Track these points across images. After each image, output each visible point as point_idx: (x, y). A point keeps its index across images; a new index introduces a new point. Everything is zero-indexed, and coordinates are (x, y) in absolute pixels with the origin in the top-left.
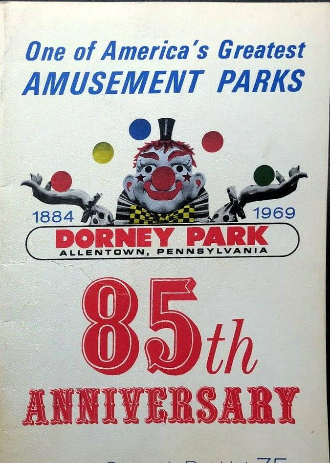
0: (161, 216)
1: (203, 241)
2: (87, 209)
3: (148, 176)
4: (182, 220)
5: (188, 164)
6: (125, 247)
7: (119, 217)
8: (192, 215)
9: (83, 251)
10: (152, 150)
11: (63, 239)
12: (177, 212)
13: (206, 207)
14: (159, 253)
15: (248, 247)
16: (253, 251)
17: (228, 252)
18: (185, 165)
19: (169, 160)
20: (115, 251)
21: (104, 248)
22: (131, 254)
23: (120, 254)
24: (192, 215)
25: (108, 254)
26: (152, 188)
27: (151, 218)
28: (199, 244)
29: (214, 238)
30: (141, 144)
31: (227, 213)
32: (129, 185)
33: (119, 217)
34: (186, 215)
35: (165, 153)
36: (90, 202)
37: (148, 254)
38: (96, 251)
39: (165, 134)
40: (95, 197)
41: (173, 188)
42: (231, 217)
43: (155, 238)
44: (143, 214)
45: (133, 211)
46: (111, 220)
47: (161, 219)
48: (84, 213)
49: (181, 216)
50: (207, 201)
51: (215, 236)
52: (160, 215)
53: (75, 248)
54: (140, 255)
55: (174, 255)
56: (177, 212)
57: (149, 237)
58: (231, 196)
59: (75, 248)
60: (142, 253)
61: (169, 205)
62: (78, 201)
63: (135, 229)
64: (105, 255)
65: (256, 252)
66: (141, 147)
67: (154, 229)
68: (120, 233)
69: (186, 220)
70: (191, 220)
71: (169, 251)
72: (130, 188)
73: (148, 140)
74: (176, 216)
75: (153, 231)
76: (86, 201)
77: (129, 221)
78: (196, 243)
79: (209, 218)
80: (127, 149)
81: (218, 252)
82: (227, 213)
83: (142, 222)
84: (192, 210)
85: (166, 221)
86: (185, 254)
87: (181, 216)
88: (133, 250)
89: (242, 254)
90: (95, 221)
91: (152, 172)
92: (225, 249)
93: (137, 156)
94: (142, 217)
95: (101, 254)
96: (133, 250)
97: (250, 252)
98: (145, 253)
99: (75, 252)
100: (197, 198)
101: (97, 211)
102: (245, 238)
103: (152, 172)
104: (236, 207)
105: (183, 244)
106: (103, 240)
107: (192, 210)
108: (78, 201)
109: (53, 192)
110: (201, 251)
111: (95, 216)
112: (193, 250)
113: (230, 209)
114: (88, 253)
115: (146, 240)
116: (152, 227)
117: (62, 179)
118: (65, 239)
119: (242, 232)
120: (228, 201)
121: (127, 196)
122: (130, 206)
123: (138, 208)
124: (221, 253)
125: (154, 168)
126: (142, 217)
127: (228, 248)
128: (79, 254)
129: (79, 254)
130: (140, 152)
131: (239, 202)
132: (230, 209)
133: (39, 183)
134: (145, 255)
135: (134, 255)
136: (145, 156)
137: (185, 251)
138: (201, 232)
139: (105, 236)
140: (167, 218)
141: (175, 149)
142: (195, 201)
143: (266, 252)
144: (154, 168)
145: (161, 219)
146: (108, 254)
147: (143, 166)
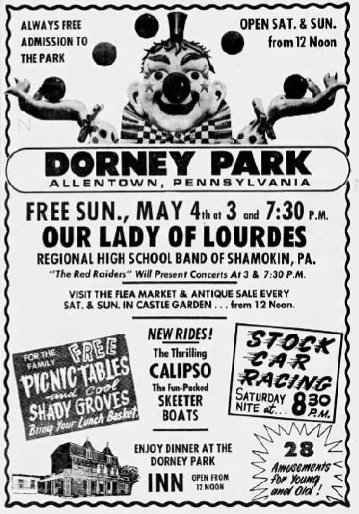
0: (176, 135)
1: (231, 168)
2: (86, 124)
3: (158, 85)
4: (200, 140)
5: (204, 70)
6: (133, 175)
8: (212, 135)
9: (80, 180)
11: (55, 163)
12: (194, 130)
13: (229, 125)
14: (175, 184)
15: (286, 177)
16: (293, 183)
17: (262, 185)
18: (202, 72)
19: (183, 62)
20: (121, 181)
21: (108, 176)
22: (140, 185)
23: (126, 185)
24: (212, 135)
25: (112, 185)
27: (164, 138)
28: (226, 173)
29: (245, 165)
30: (149, 43)
32: (136, 94)
33: (124, 136)
34: (205, 135)
35: (177, 54)
36: (88, 116)
37: (162, 186)
38: (96, 181)
39: (177, 32)
40: (95, 110)
41: (189, 99)
42: (259, 137)
43: (171, 165)
44: (154, 132)
45: (141, 128)
46: (116, 139)
47: (175, 139)
48: (81, 131)
50: (228, 117)
51: (245, 162)
52: (173, 134)
53: (70, 175)
54: (152, 187)
55: (195, 187)
56: (194, 131)
57: (163, 163)
58: (257, 112)
59: (70, 175)
60: (155, 185)
61: (183, 122)
62: (73, 115)
63: (145, 152)
64: (107, 186)
65: (296, 184)
66: (149, 47)
67: (171, 153)
68: (127, 156)
69: (205, 141)
70: (211, 140)
71: (188, 182)
72: (137, 98)
74: (193, 136)
75: (168, 155)
77: (136, 141)
78: (222, 171)
79: (233, 139)
80: (132, 49)
81: (249, 185)
82: (254, 133)
83: (152, 142)
84: (211, 128)
85: (181, 142)
86: (208, 187)
87: (199, 135)
88: (142, 181)
89: (279, 187)
90: (96, 140)
92: (259, 180)
94: (153, 137)
95: (102, 185)
96: (142, 181)
97: (289, 184)
98: (159, 185)
99: (69, 182)
101: (97, 128)
102: (283, 166)
103: (162, 79)
105: (207, 174)
106: (105, 164)
107: (211, 128)
108: (73, 115)
109: (44, 103)
110: (228, 182)
112: (218, 180)
113: (257, 127)
114: (86, 183)
115: (160, 167)
116: (167, 150)
117: (53, 88)
118: (57, 164)
119: (279, 158)
120: (255, 117)
121: (132, 107)
122: (137, 122)
123: (148, 125)
124: (253, 185)
125: (165, 75)
126: (153, 137)
127: (262, 178)
128: (75, 186)
129: (75, 186)
130: (148, 54)
131: (268, 118)
132: (257, 127)
133: (27, 90)
134: (158, 188)
135: (144, 186)
136: (155, 59)
137: (208, 182)
138: (228, 156)
139: (108, 160)
140: (182, 137)
141: (190, 51)
143: (308, 184)
144: (165, 75)
145: (175, 139)
146: (112, 185)
147: (151, 71)
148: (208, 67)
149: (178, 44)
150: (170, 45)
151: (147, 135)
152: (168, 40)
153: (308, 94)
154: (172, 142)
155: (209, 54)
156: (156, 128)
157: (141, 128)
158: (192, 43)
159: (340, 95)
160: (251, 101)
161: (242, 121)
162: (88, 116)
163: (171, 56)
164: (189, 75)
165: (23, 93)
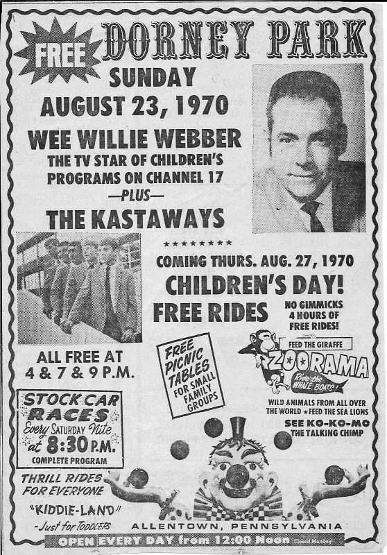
3: (223, 474)
7: (196, 515)
8: (267, 514)
10: (226, 448)
18: (258, 464)
19: (242, 458)
24: (267, 514)
26: (228, 485)
30: (216, 441)
31: (301, 512)
32: (205, 482)
33: (196, 515)
34: (261, 514)
35: (238, 450)
36: (167, 500)
39: (238, 433)
40: (172, 494)
41: (248, 486)
42: (305, 516)
45: (210, 509)
47: (238, 517)
49: (256, 514)
52: (236, 513)
62: (154, 499)
70: (266, 518)
73: (222, 437)
74: (251, 515)
76: (163, 499)
79: (284, 517)
80: (201, 445)
82: (301, 512)
83: (218, 519)
84: (266, 509)
87: (256, 514)
91: (226, 470)
93: (212, 454)
100: (270, 496)
103: (226, 470)
104: (310, 505)
107: (266, 509)
108: (154, 499)
109: (131, 489)
111: (173, 514)
120: (302, 500)
125: (228, 466)
126: (219, 515)
131: (312, 500)
132: (302, 509)
133: (117, 479)
136: (219, 454)
141: (248, 447)
142: (268, 500)
144: (228, 466)
145: (238, 517)
148: (263, 460)
149: (239, 442)
150: (232, 443)
151: (214, 514)
152: (231, 439)
153: (345, 481)
154: (234, 520)
155: (264, 449)
156: (221, 509)
157: (210, 509)
158: (249, 441)
159: (369, 482)
160: (298, 486)
161: (290, 503)
162: (167, 500)
163: (233, 451)
164: (248, 466)
165: (115, 482)
